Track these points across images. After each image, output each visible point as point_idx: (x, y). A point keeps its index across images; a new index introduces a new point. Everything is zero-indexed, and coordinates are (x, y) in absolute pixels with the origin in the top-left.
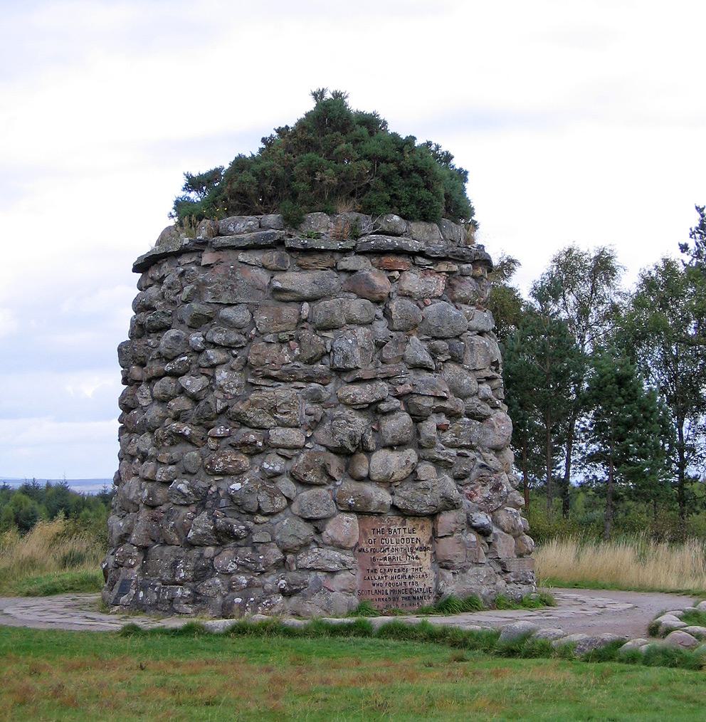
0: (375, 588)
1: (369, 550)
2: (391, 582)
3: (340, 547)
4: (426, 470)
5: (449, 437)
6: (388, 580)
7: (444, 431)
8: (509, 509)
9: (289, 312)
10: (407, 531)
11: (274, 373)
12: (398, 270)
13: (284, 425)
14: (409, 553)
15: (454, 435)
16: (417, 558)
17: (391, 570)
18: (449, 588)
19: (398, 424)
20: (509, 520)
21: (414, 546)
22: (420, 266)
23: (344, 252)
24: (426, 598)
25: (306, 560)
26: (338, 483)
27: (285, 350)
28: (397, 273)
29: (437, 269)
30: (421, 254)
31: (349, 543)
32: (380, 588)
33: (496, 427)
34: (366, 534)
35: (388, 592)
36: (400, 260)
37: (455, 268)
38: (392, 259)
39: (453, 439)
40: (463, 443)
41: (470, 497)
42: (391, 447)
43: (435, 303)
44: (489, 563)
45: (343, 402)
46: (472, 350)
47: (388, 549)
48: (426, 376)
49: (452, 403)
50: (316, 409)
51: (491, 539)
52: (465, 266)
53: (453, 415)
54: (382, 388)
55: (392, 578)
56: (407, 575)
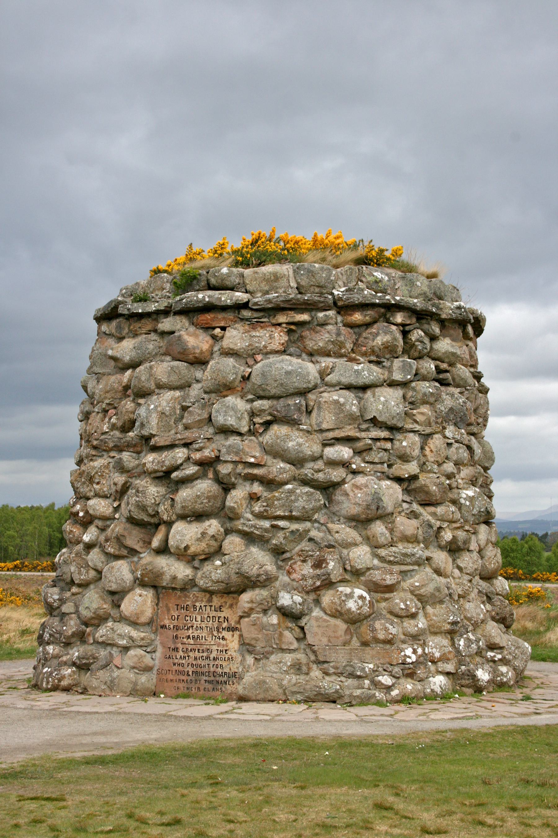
0: (176, 668)
1: (172, 626)
2: (194, 663)
3: (134, 624)
4: (233, 543)
5: (257, 508)
6: (191, 661)
7: (258, 499)
8: (340, 589)
10: (213, 608)
12: (219, 327)
13: (97, 495)
14: (215, 633)
15: (265, 504)
16: (223, 638)
17: (195, 650)
18: (249, 674)
20: (332, 603)
21: (221, 625)
22: (247, 320)
23: (166, 312)
24: (231, 682)
25: (102, 632)
26: (142, 555)
28: (218, 331)
29: (274, 321)
30: (245, 306)
31: (138, 618)
32: (181, 668)
33: (351, 494)
34: (169, 610)
35: (190, 673)
36: (220, 316)
37: (305, 317)
38: (209, 316)
39: (262, 509)
40: (278, 513)
41: (289, 573)
43: (269, 358)
44: (305, 650)
45: (145, 473)
46: (319, 408)
47: (192, 627)
48: (234, 440)
49: (278, 468)
50: (120, 479)
51: (303, 622)
52: (321, 315)
53: (270, 483)
54: (180, 454)
55: (196, 659)
56: (212, 656)
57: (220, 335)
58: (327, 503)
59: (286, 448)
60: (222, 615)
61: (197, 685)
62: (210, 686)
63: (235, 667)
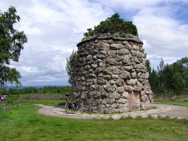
4: (138, 83)
5: (142, 76)
9: (114, 51)
11: (112, 63)
19: (134, 74)
25: (120, 101)
27: (114, 59)
42: (133, 78)
45: (125, 69)
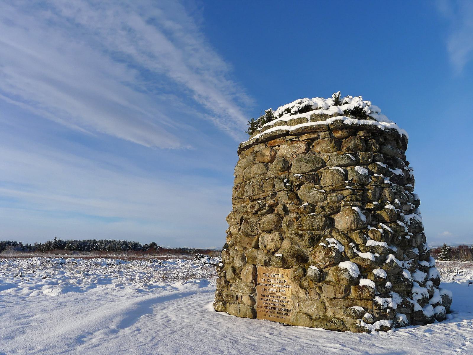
14: (281, 288)
28: (277, 147)
35: (271, 308)
36: (277, 140)
47: (271, 284)
57: (278, 149)
58: (331, 222)
59: (308, 196)
60: (283, 279)
61: (274, 315)
62: (279, 316)
63: (290, 307)
